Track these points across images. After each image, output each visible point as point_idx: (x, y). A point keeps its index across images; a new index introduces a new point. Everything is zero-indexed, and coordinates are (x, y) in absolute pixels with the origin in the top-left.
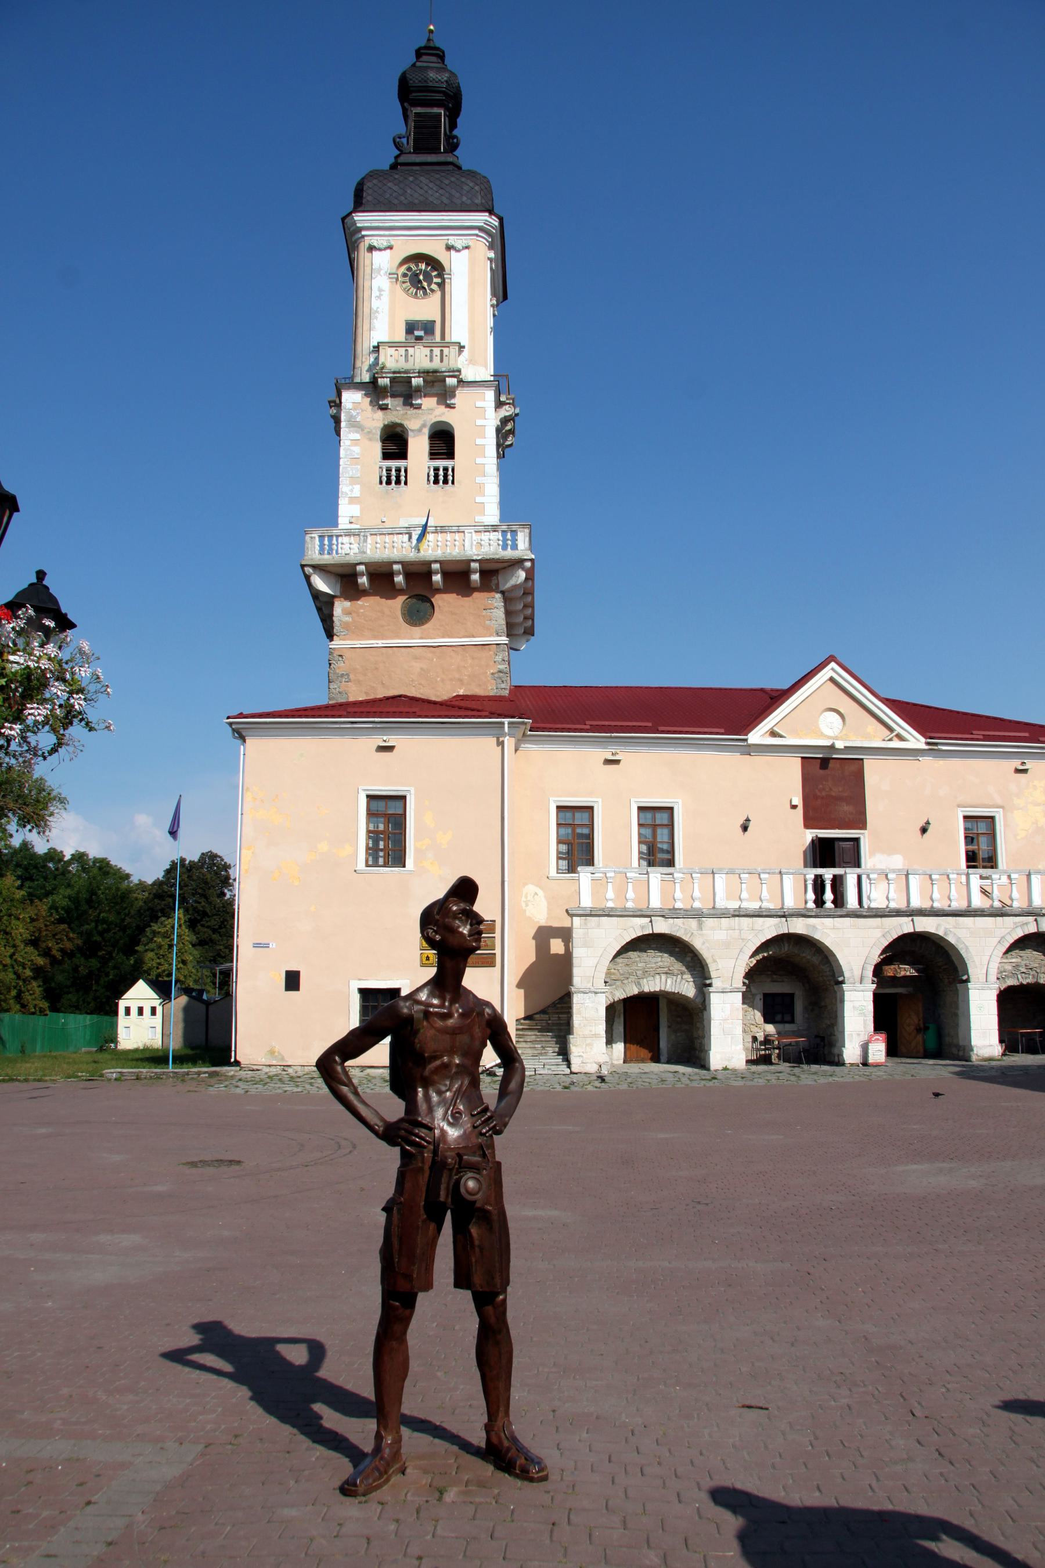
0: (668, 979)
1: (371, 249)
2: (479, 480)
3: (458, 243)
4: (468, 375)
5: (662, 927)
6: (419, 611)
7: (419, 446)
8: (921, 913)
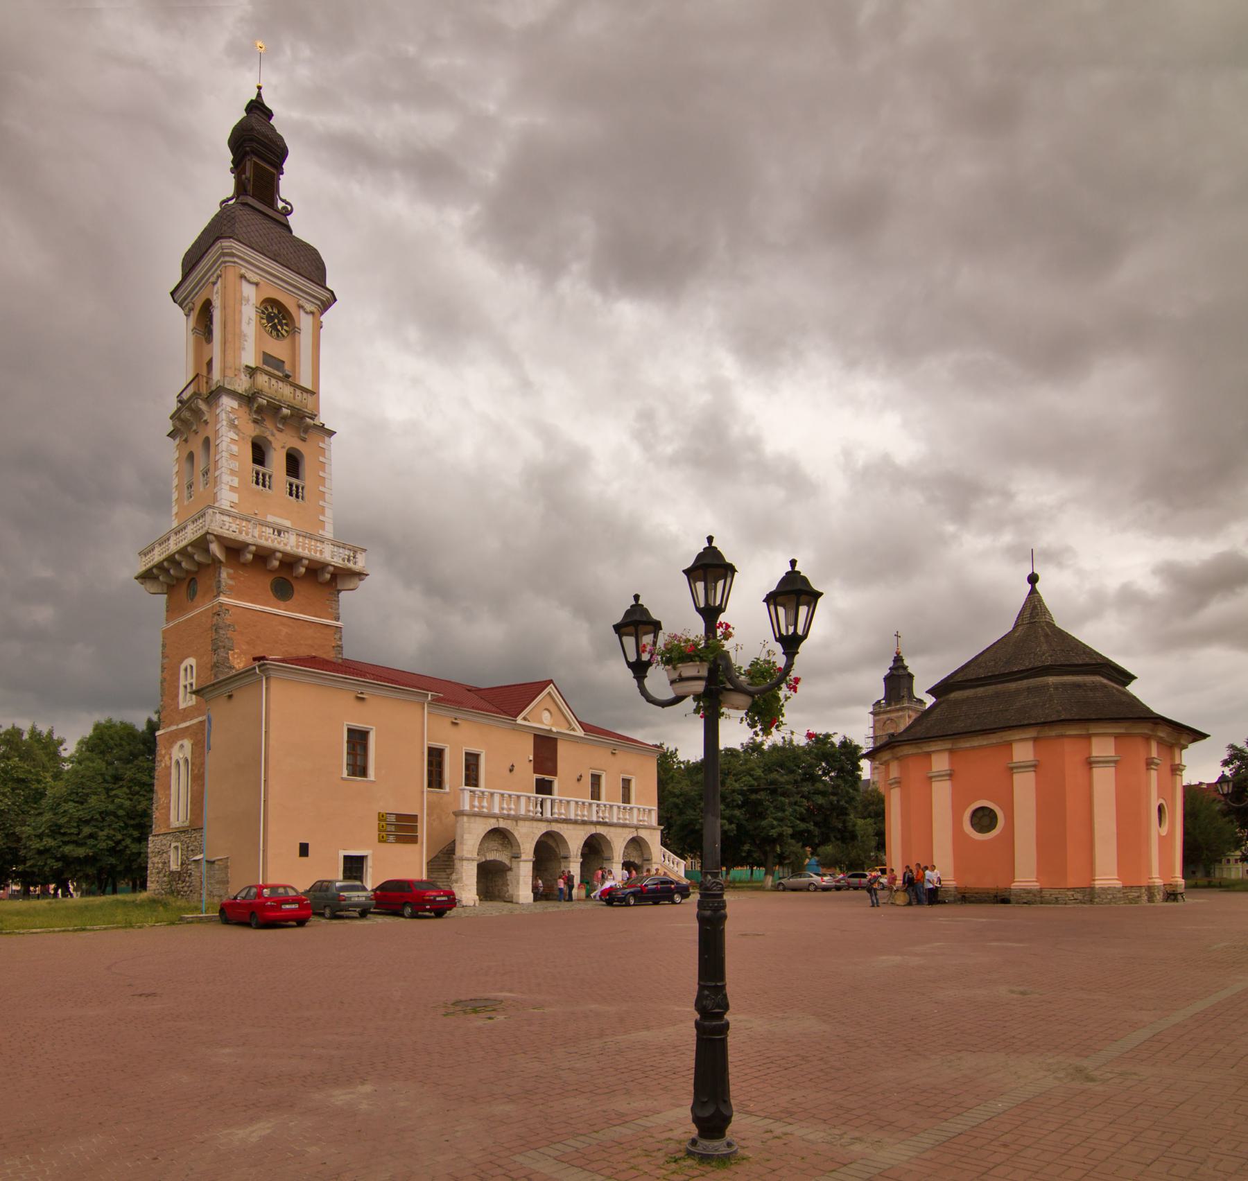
0: (497, 855)
5: (502, 824)
6: (282, 590)
7: (277, 462)
8: (598, 823)
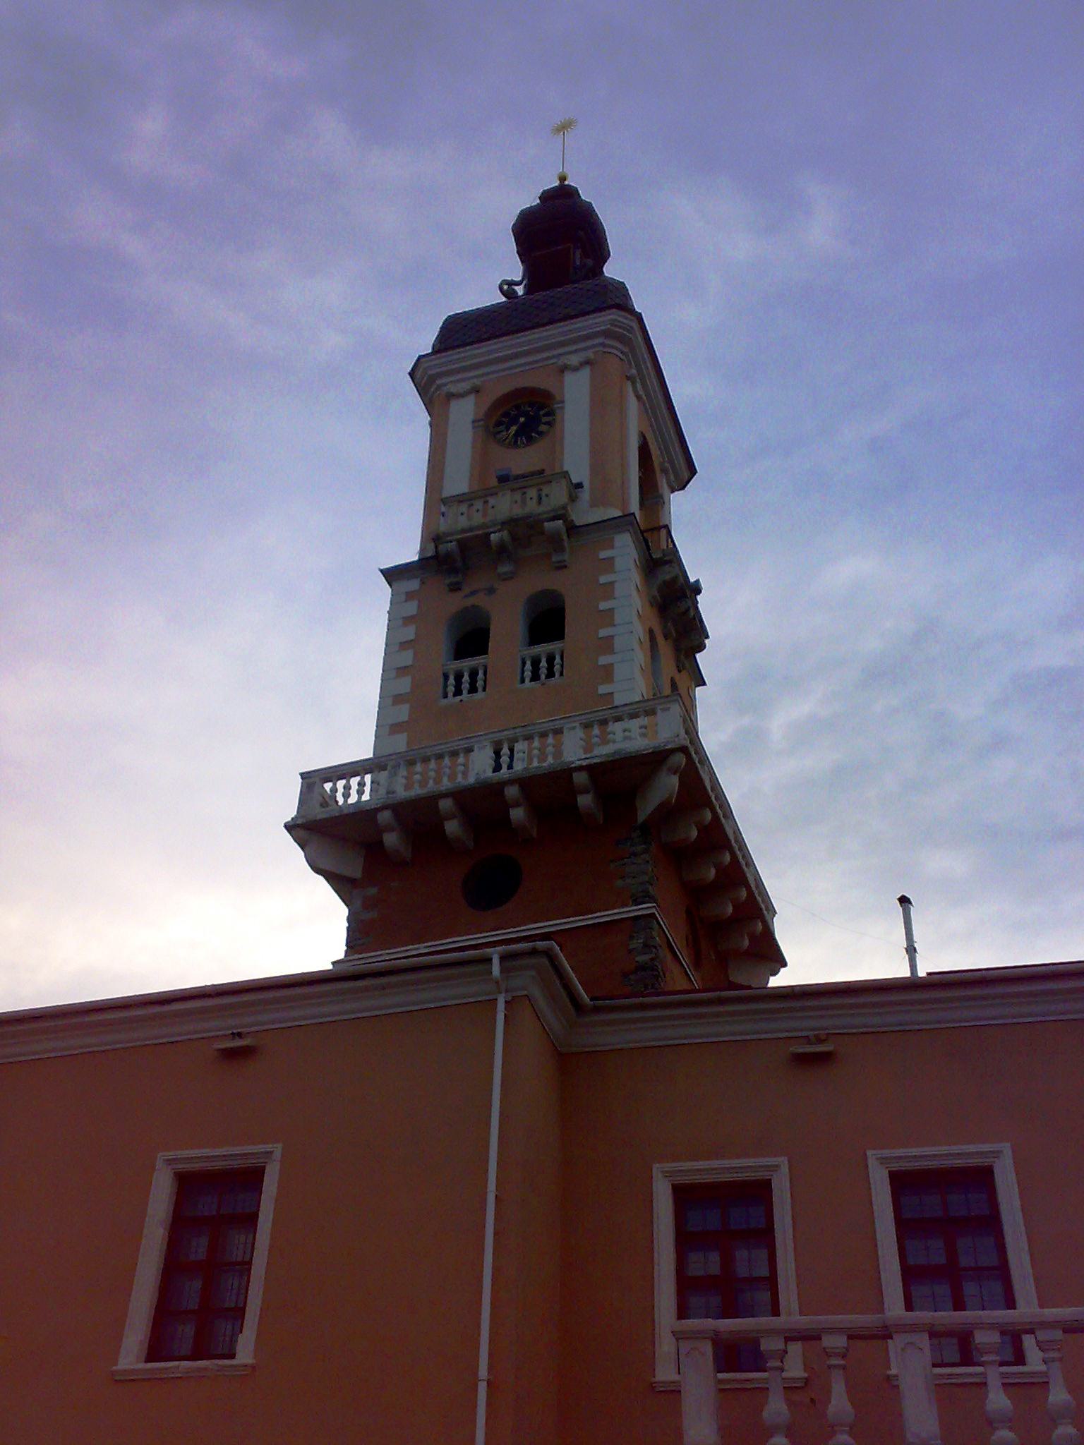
1: (451, 396)
2: (603, 660)
3: (574, 360)
4: (584, 514)
